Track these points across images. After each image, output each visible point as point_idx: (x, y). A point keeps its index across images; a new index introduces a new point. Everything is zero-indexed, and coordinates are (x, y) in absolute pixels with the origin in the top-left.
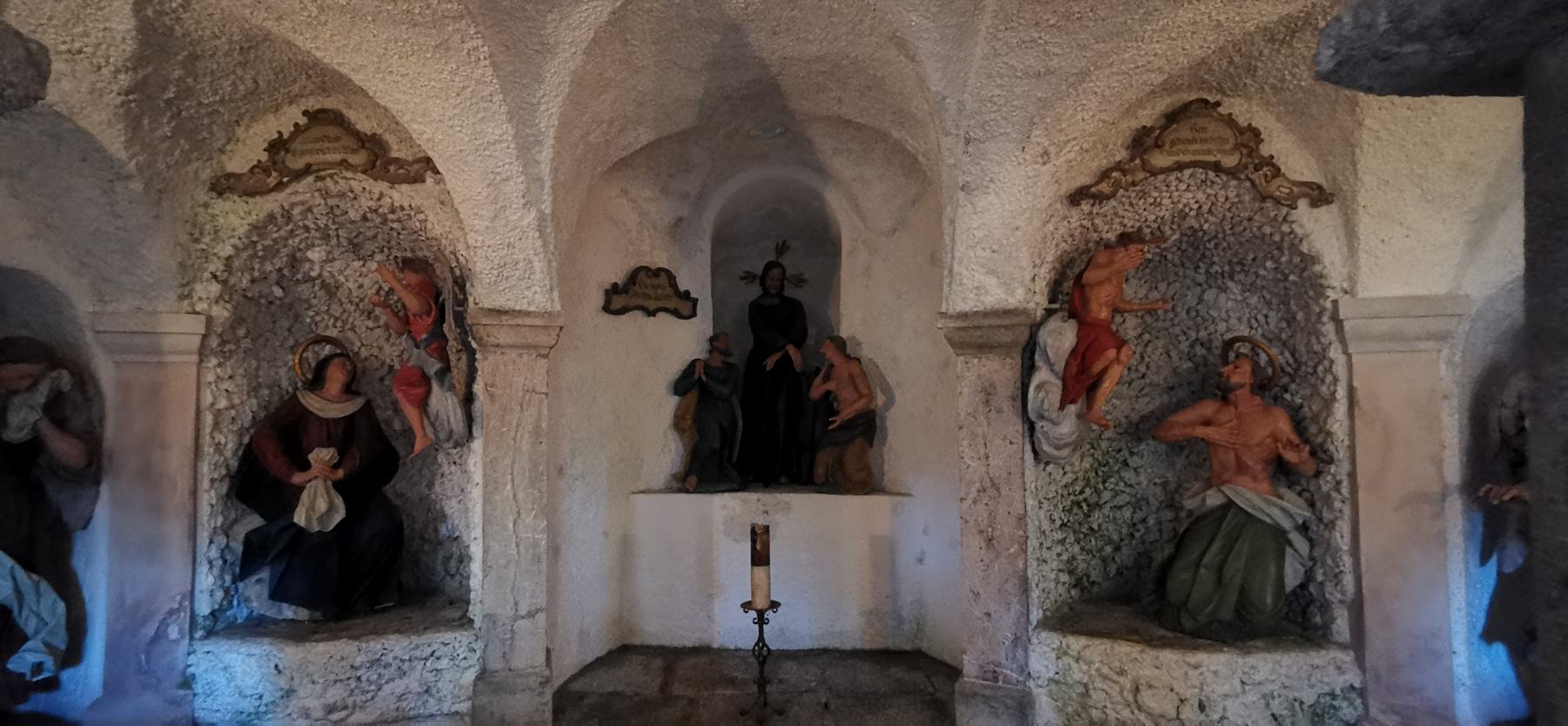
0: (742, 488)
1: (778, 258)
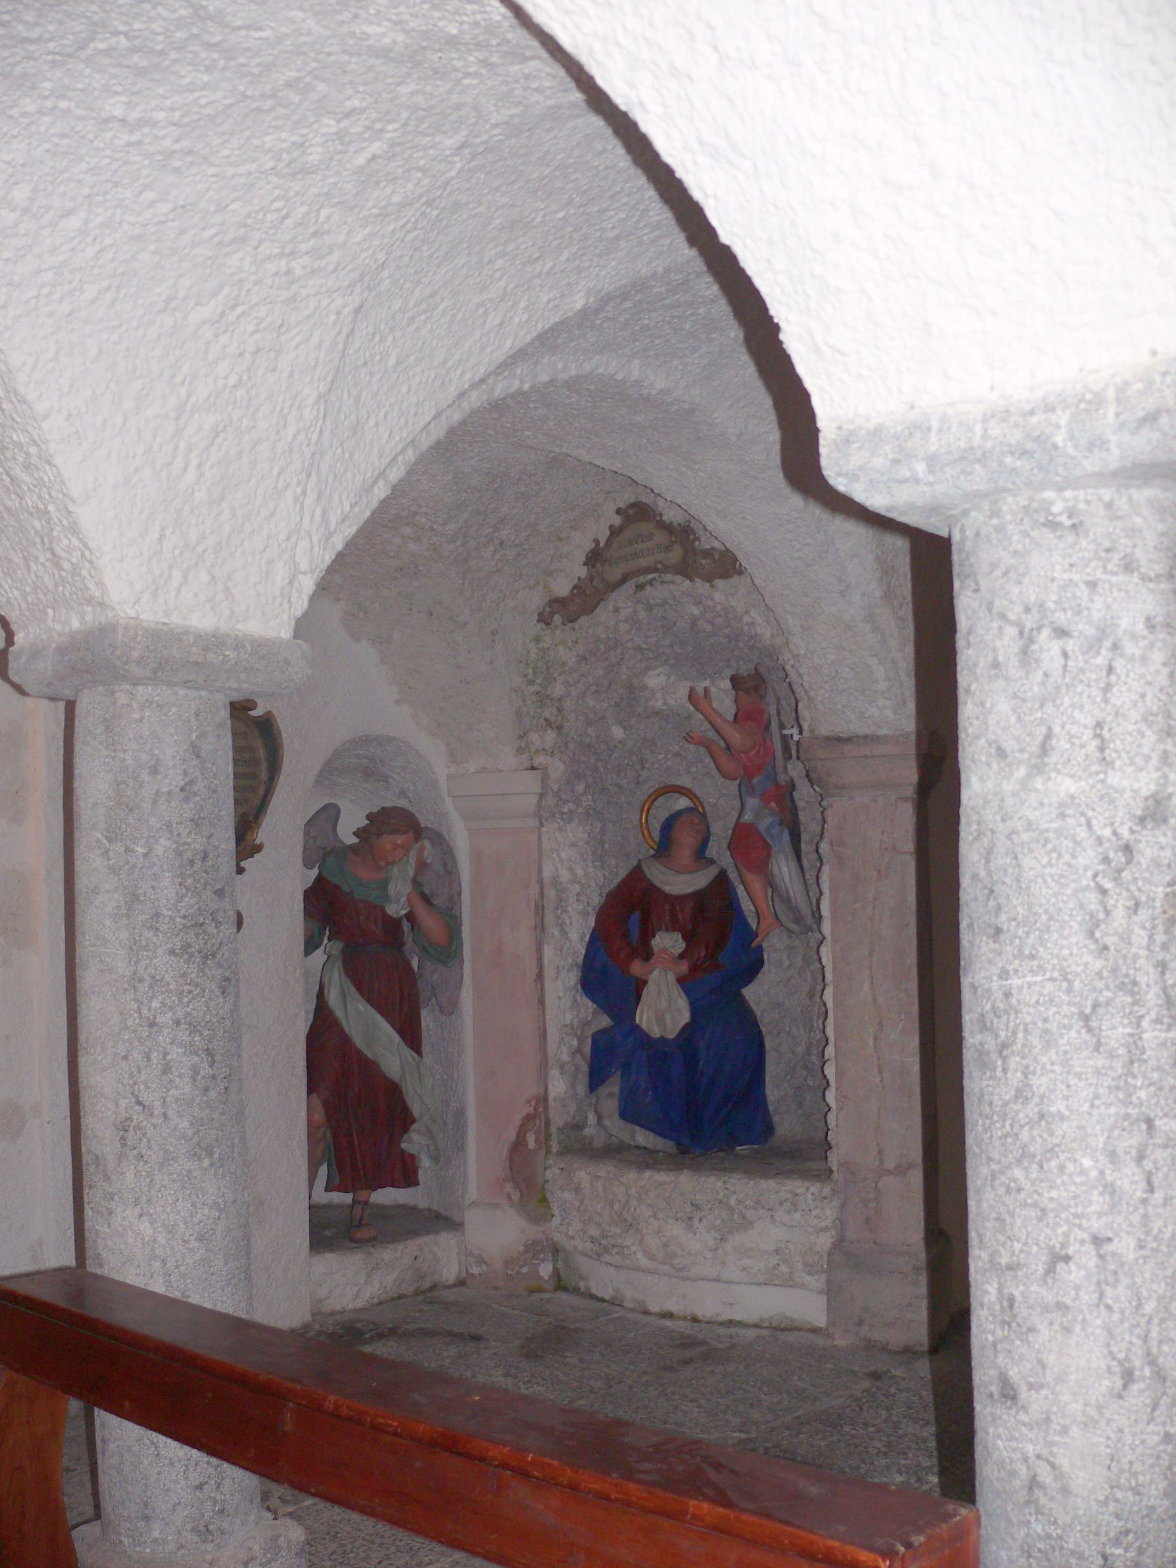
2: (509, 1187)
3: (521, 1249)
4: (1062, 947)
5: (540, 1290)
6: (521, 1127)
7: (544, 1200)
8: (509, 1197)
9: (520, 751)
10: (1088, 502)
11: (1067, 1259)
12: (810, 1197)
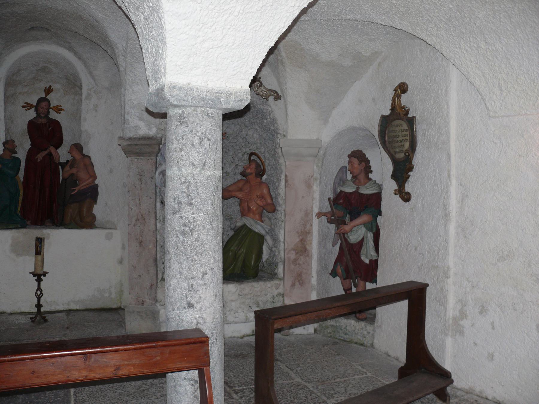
0: (23, 227)
1: (46, 96)
4: (207, 207)
10: (215, 112)
11: (206, 274)
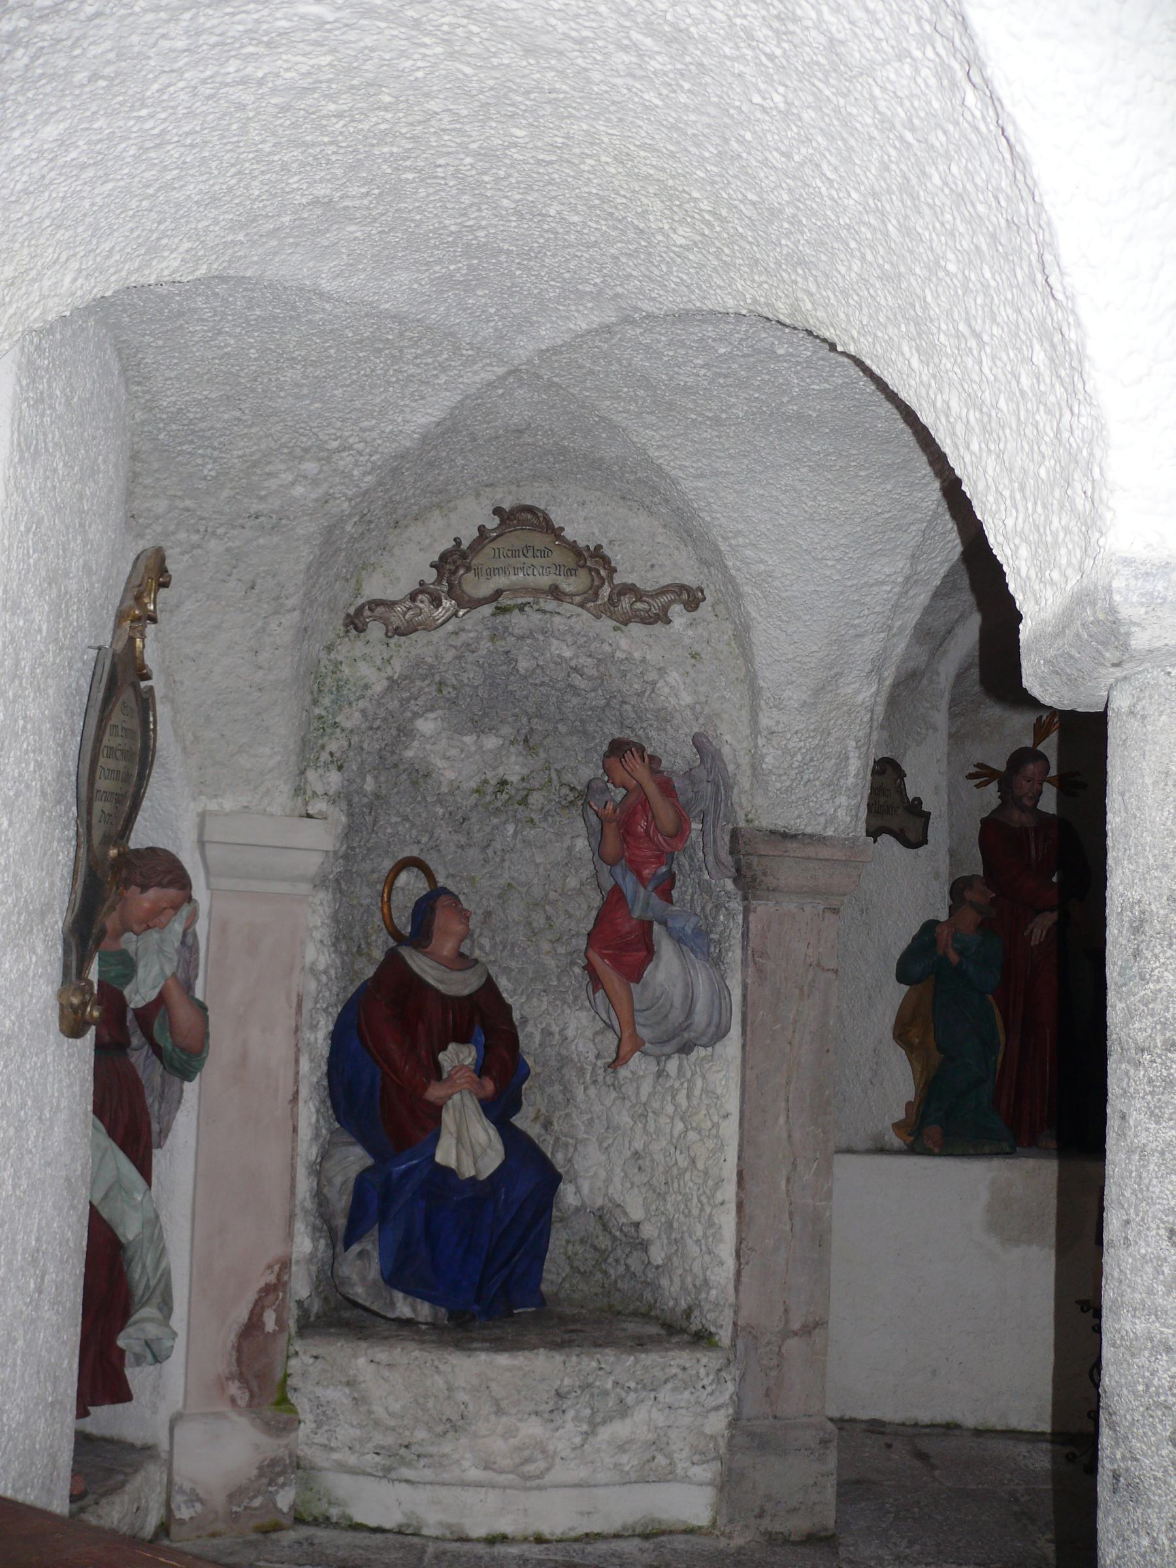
1: (1036, 743)
2: (234, 1388)
3: (255, 1472)
5: (277, 1528)
6: (256, 1303)
7: (283, 1401)
8: (233, 1400)
9: (299, 791)
12: (702, 1371)
